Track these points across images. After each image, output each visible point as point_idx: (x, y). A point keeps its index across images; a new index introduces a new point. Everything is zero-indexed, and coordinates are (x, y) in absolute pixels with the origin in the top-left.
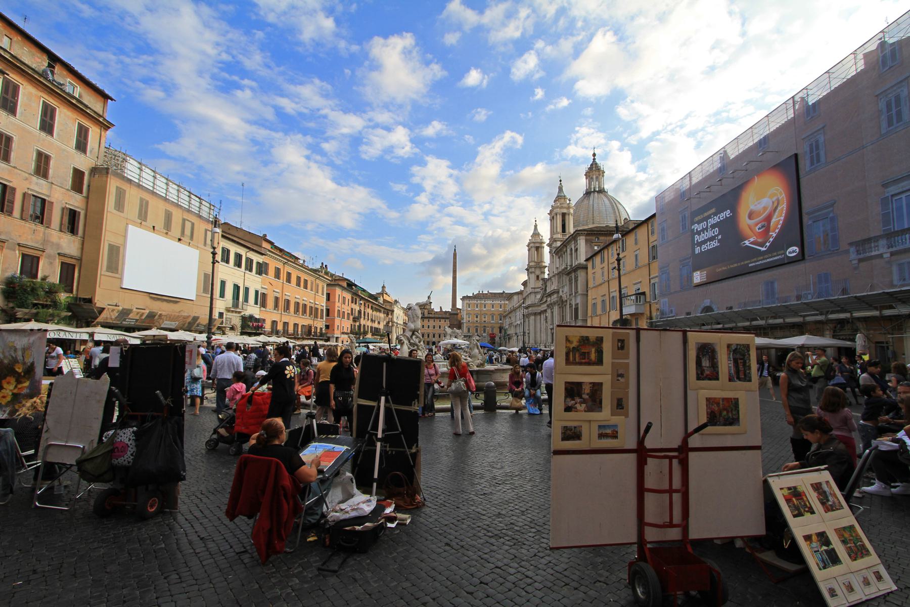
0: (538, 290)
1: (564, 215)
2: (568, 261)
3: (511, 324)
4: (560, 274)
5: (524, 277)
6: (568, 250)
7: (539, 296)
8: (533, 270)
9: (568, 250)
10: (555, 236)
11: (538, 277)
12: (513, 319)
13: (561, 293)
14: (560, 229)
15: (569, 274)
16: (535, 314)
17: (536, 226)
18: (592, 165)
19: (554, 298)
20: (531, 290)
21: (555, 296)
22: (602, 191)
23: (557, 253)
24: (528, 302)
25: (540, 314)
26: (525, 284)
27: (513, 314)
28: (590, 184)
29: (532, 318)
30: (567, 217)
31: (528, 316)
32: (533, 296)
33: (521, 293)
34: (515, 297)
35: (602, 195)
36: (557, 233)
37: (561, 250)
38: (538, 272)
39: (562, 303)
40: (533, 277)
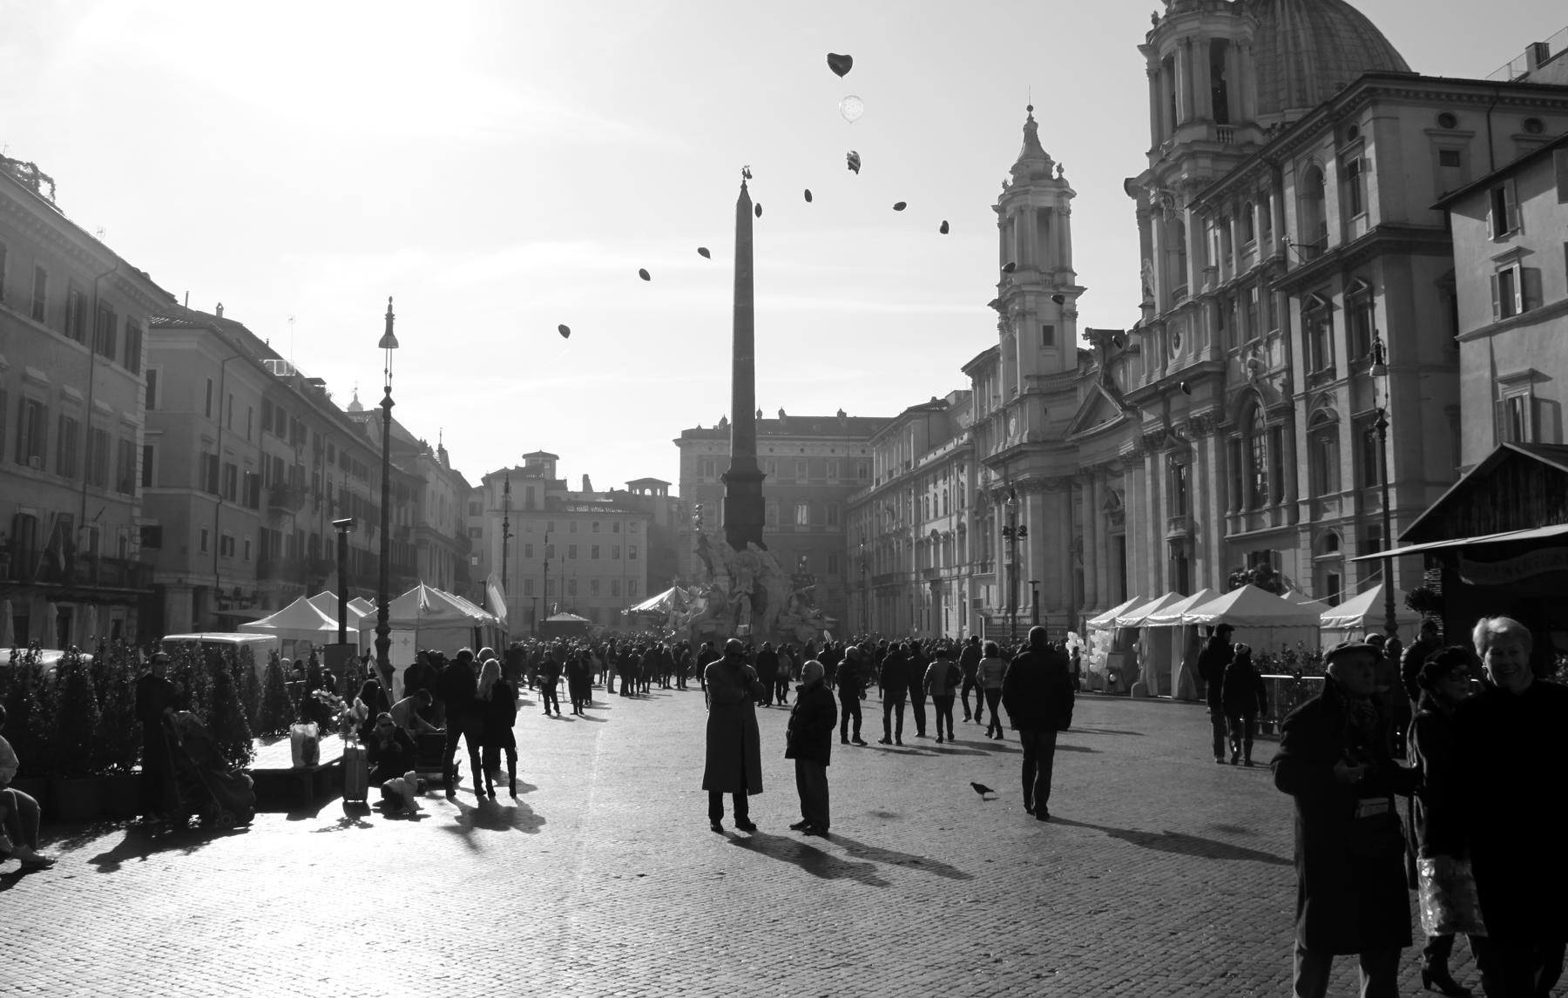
1: (1218, 48)
4: (1223, 301)
5: (986, 334)
11: (1048, 334)
14: (1205, 107)
15: (1298, 285)
17: (1031, 130)
26: (980, 368)
30: (1231, 58)
33: (934, 409)
36: (1192, 121)
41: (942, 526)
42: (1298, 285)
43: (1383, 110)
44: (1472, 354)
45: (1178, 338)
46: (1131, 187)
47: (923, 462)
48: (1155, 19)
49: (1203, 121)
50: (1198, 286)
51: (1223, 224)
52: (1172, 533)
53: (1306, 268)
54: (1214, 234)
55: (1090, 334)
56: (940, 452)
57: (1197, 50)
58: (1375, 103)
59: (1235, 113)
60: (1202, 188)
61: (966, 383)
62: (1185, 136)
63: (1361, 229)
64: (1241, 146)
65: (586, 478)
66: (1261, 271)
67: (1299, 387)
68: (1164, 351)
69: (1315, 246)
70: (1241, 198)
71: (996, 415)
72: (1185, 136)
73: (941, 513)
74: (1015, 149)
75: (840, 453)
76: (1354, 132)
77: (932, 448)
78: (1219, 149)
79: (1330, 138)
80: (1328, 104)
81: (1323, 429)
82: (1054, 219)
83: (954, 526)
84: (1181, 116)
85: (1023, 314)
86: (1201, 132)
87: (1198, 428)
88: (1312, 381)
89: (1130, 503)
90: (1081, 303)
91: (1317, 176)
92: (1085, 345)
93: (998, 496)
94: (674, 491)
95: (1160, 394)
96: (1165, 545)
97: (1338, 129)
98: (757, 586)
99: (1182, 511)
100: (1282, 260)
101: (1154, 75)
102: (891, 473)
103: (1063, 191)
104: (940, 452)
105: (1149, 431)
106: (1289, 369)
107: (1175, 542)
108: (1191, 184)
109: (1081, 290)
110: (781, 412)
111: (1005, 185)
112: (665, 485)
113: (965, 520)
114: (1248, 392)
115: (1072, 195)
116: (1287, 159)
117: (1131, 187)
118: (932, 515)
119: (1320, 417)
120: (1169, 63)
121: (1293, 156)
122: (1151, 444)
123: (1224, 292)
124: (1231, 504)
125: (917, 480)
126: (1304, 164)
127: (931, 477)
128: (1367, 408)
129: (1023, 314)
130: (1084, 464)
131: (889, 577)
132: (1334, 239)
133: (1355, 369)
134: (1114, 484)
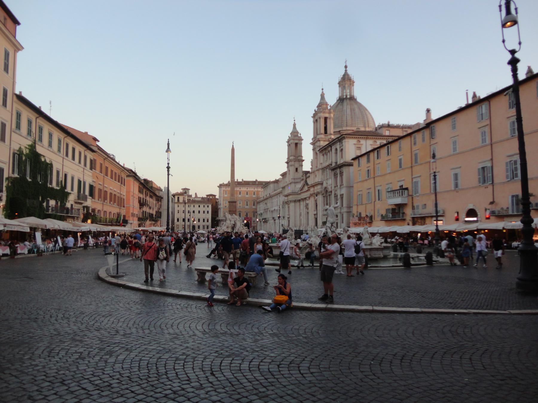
0: (299, 180)
2: (332, 158)
3: (266, 210)
4: (323, 169)
5: (284, 169)
6: (333, 150)
7: (299, 186)
8: (292, 163)
9: (333, 150)
10: (319, 137)
11: (297, 169)
12: (269, 205)
13: (325, 185)
14: (323, 131)
15: (333, 169)
16: (295, 201)
17: (294, 125)
18: (344, 75)
19: (318, 189)
20: (291, 181)
21: (319, 187)
22: (352, 98)
23: (321, 150)
24: (288, 191)
25: (299, 201)
26: (284, 175)
27: (268, 201)
28: (342, 91)
29: (292, 205)
30: (328, 121)
31: (287, 203)
32: (293, 185)
33: (277, 182)
34: (272, 186)
35: (352, 102)
37: (325, 149)
38: (297, 165)
39: (326, 193)
40: (293, 169)
41: (276, 208)
42: (333, 169)
44: (355, 186)
48: (315, 111)
51: (323, 155)
54: (322, 157)
56: (276, 192)
57: (321, 119)
59: (328, 132)
63: (342, 162)
65: (196, 194)
66: (328, 166)
67: (333, 188)
69: (336, 163)
72: (319, 137)
74: (291, 130)
75: (256, 189)
77: (275, 190)
79: (338, 143)
80: (338, 138)
81: (336, 196)
82: (298, 145)
84: (318, 132)
85: (291, 165)
88: (335, 187)
89: (310, 206)
90: (303, 163)
91: (336, 149)
93: (286, 203)
94: (217, 197)
95: (313, 186)
100: (331, 165)
101: (314, 122)
103: (301, 139)
104: (276, 192)
107: (315, 215)
108: (320, 146)
109: (304, 160)
112: (215, 196)
113: (281, 207)
114: (326, 188)
115: (302, 140)
120: (317, 120)
122: (311, 195)
123: (323, 169)
125: (271, 197)
126: (335, 148)
128: (342, 193)
129: (291, 165)
131: (265, 219)
132: (338, 163)
133: (341, 186)
134: (307, 202)
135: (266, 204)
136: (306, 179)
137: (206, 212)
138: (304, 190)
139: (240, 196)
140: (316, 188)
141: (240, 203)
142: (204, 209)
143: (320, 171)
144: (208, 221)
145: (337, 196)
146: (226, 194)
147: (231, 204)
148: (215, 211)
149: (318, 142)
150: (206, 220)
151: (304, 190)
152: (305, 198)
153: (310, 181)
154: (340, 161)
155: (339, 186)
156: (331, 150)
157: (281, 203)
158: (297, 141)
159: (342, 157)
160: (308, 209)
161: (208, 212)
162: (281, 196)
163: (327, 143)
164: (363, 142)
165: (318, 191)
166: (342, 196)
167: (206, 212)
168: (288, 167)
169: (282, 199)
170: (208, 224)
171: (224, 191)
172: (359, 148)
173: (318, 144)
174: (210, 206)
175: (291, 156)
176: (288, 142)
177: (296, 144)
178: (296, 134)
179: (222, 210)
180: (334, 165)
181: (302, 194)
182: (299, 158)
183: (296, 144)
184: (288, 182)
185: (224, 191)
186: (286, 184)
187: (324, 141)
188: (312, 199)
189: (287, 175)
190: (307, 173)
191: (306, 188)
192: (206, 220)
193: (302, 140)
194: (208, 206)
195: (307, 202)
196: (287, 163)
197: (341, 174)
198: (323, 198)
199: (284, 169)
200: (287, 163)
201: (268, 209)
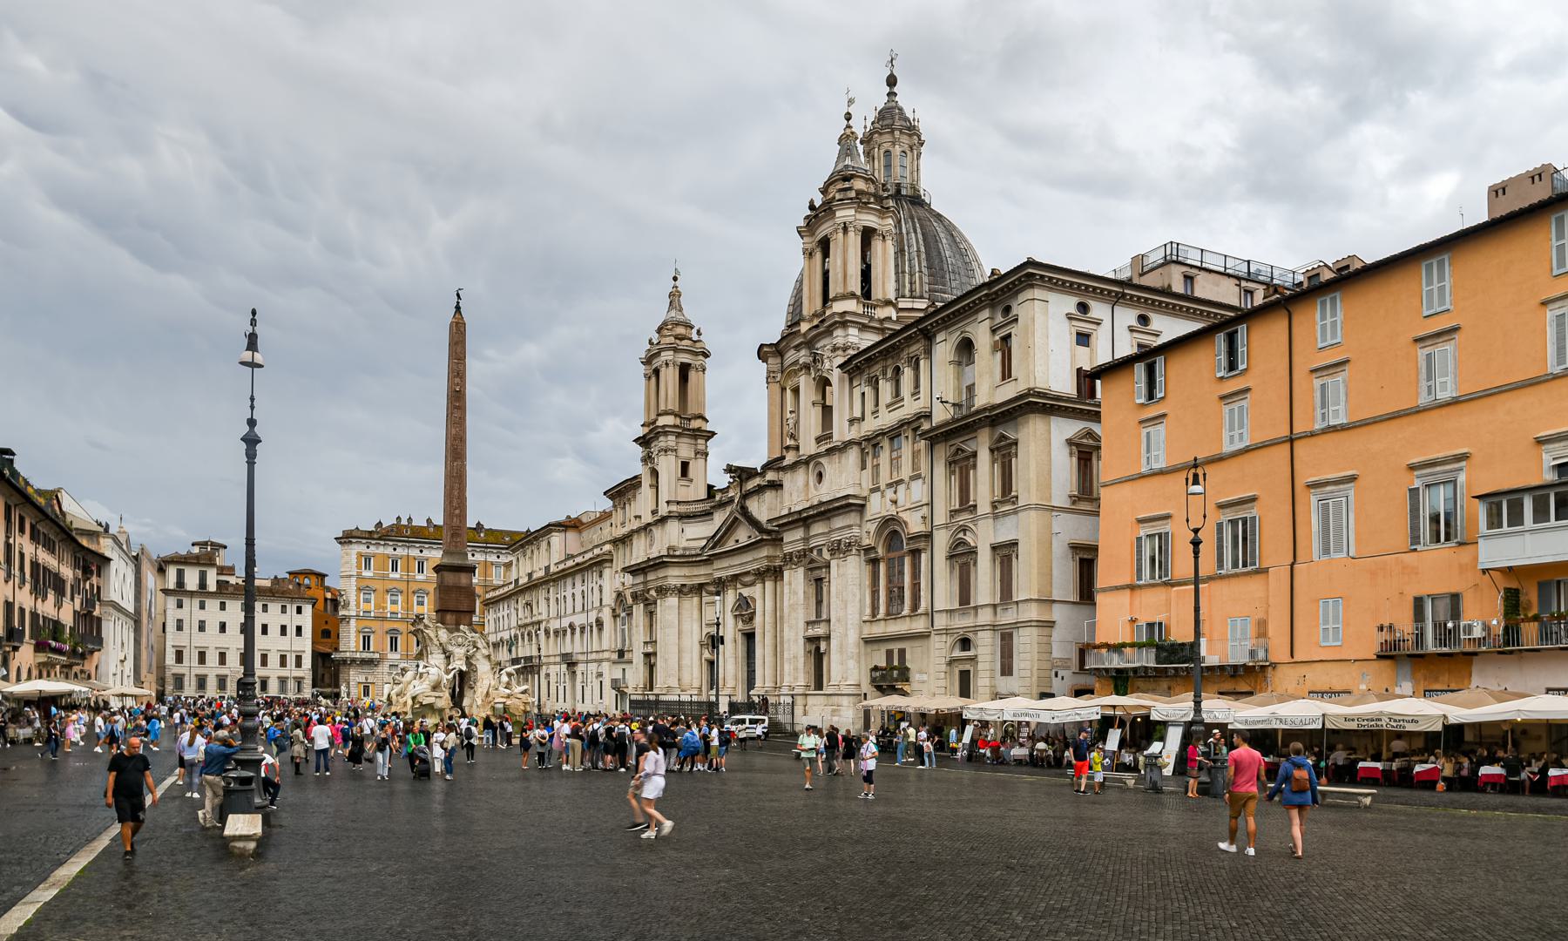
0: (700, 507)
2: (936, 386)
3: (531, 629)
4: (870, 444)
5: (631, 463)
11: (685, 466)
12: (542, 610)
14: (855, 286)
16: (681, 591)
20: (664, 510)
26: (622, 492)
30: (877, 244)
32: (673, 527)
39: (896, 547)
40: (667, 467)
41: (579, 620)
43: (1037, 293)
45: (820, 475)
46: (763, 353)
47: (561, 567)
49: (853, 295)
50: (841, 433)
52: (811, 632)
53: (954, 421)
55: (730, 469)
58: (1032, 286)
59: (877, 293)
60: (852, 352)
61: (607, 504)
62: (838, 307)
63: (1008, 392)
64: (881, 321)
66: (903, 424)
67: (940, 518)
68: (807, 484)
70: (890, 361)
71: (638, 531)
72: (838, 307)
73: (579, 608)
74: (661, 313)
76: (1007, 310)
78: (865, 321)
79: (986, 313)
81: (962, 556)
82: (692, 375)
83: (592, 619)
86: (851, 305)
87: (839, 549)
91: (966, 348)
92: (722, 480)
95: (803, 520)
96: (802, 641)
97: (993, 306)
98: (468, 659)
99: (818, 613)
100: (928, 416)
102: (530, 575)
105: (787, 549)
106: (931, 504)
109: (714, 434)
110: (429, 521)
111: (651, 342)
112: (322, 576)
113: (606, 615)
115: (706, 355)
116: (939, 331)
117: (763, 353)
118: (570, 611)
119: (963, 543)
121: (946, 328)
123: (868, 440)
124: (868, 611)
127: (569, 581)
130: (717, 575)
133: (994, 505)
135: (528, 604)
136: (746, 496)
137: (291, 631)
138: (730, 545)
139: (420, 577)
140: (818, 528)
141: (421, 603)
142: (285, 619)
143: (853, 455)
144: (299, 663)
145: (973, 552)
146: (368, 566)
147: (450, 578)
148: (326, 632)
149: (839, 332)
150: (291, 660)
151: (730, 545)
152: (735, 578)
153: (762, 509)
154: (990, 392)
155: (984, 507)
156: (929, 353)
157: (609, 599)
158: (684, 358)
159: (1006, 373)
160: (751, 618)
161: (299, 629)
162: (607, 572)
163: (876, 338)
164: (1099, 310)
165: (835, 537)
166: (1005, 552)
167: (291, 631)
168: (647, 459)
169: (612, 581)
170: (298, 673)
171: (360, 555)
172: (1083, 339)
173: (839, 337)
174: (308, 609)
175: (666, 413)
176: (648, 361)
177: (684, 370)
178: (681, 330)
179: (353, 622)
180: (941, 415)
181: (718, 564)
182: (695, 424)
183: (684, 370)
184: (648, 518)
185: (360, 555)
186: (635, 525)
187: (863, 328)
188: (795, 579)
189: (646, 491)
190: (741, 474)
191: (743, 535)
192: (291, 660)
193: (706, 355)
194: (299, 611)
195: (746, 592)
196: (644, 441)
197: (1005, 452)
198: (868, 569)
199: (631, 463)
200: (644, 441)
201: (539, 623)
